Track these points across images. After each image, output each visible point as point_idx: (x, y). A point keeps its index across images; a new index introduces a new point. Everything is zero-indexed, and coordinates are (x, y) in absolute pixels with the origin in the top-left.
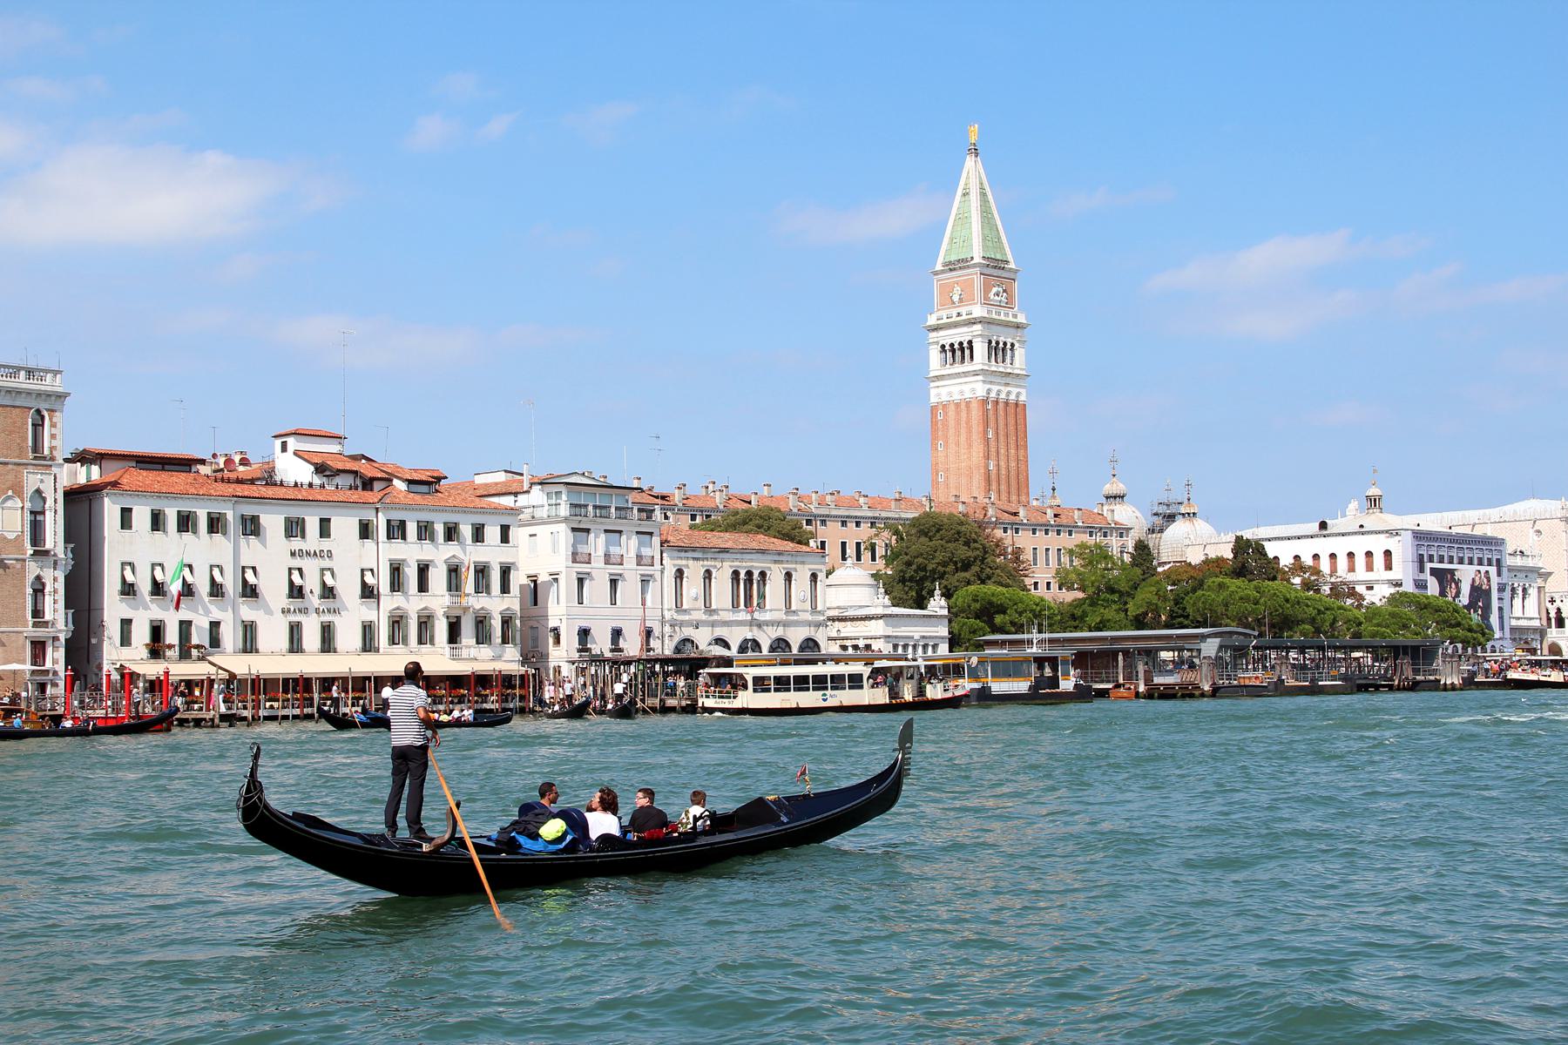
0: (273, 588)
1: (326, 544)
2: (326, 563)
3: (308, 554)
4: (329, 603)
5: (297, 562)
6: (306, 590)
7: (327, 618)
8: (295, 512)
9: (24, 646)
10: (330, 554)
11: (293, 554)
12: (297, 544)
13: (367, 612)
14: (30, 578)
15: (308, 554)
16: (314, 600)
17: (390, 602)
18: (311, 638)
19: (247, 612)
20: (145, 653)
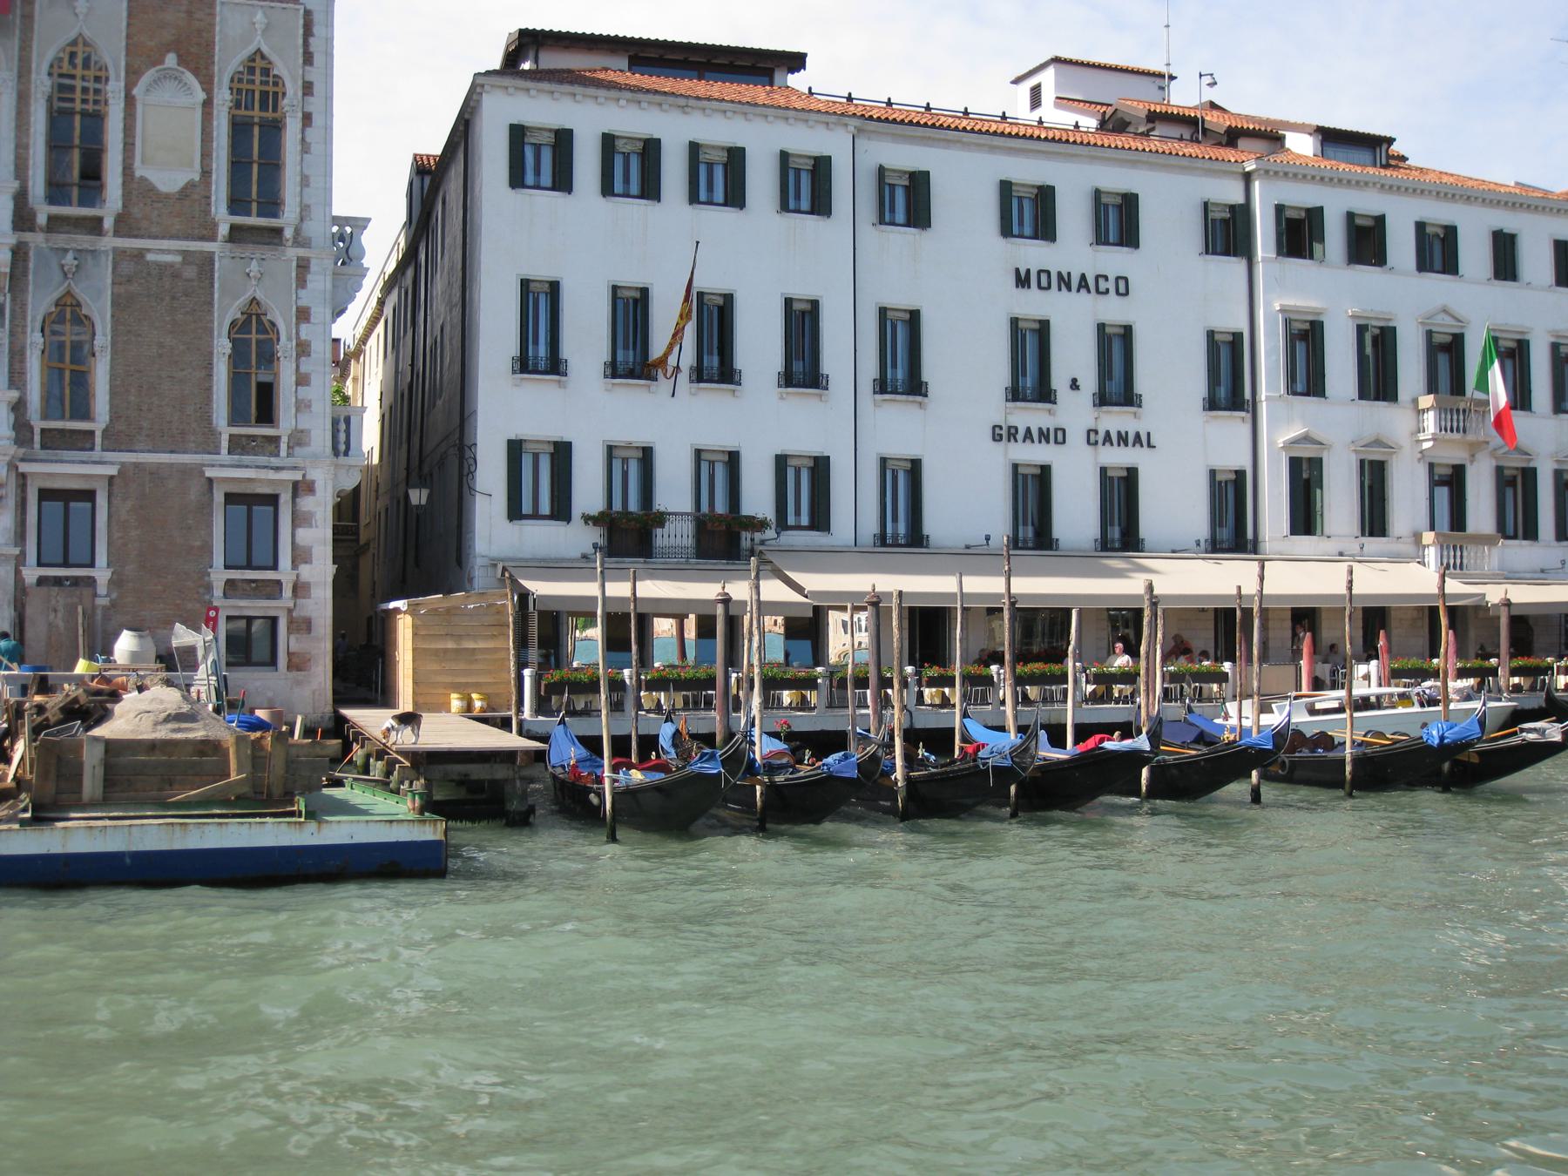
0: (966, 361)
1: (1114, 260)
2: (1113, 311)
3: (1064, 282)
4: (1116, 420)
5: (1033, 305)
6: (1059, 381)
7: (1117, 457)
8: (1028, 171)
9: (206, 507)
10: (1123, 287)
11: (1022, 280)
12: (1033, 254)
13: (1225, 444)
14: (225, 312)
15: (1064, 282)
16: (1075, 410)
17: (1283, 423)
18: (1076, 511)
19: (897, 429)
20: (595, 535)
